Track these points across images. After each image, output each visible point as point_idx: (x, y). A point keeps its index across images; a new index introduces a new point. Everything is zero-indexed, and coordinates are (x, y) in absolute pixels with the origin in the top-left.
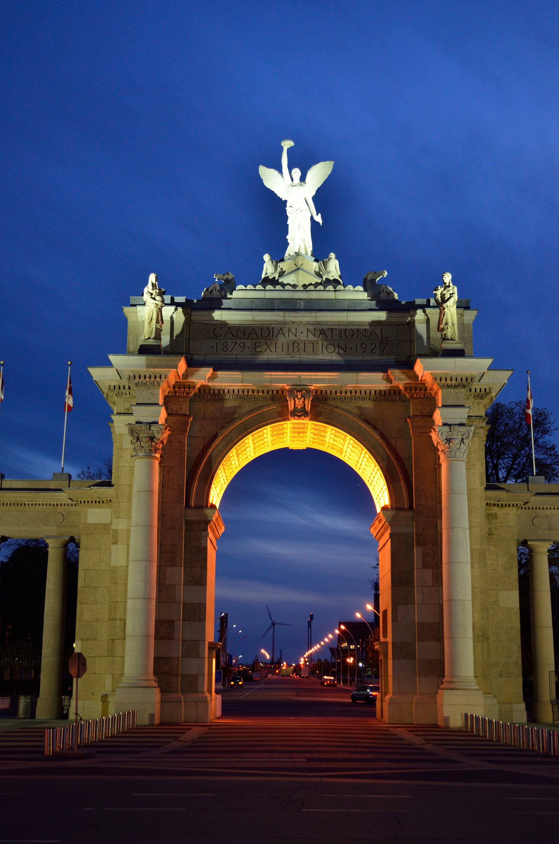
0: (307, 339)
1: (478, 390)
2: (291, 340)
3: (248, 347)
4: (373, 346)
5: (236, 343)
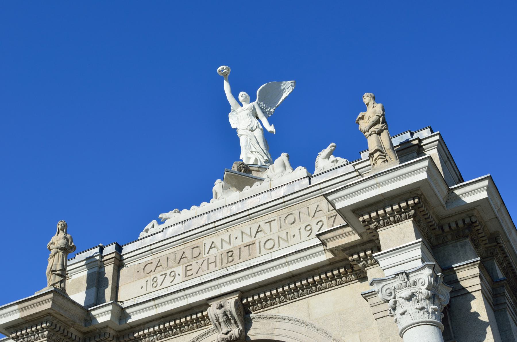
0: (242, 243)
1: (453, 226)
2: (226, 250)
3: (179, 275)
4: (320, 224)
5: (167, 273)
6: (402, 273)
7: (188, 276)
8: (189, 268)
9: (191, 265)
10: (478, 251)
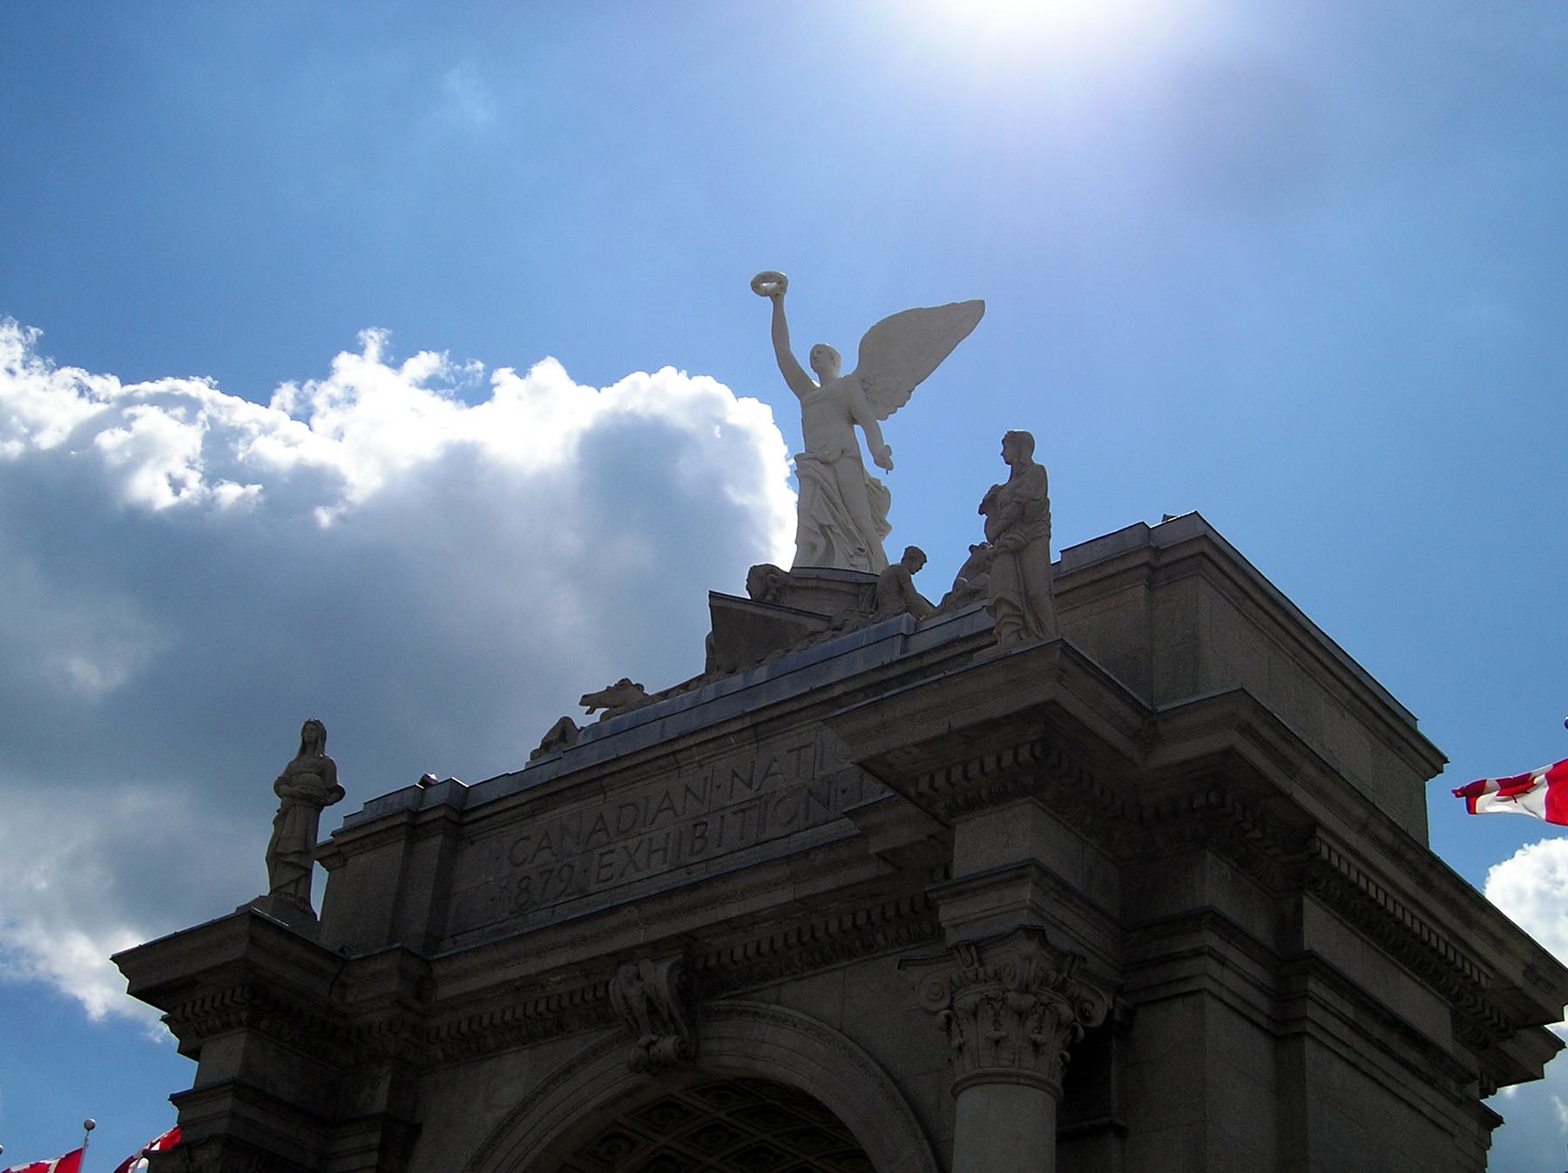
6: (968, 947)
7: (603, 881)
8: (606, 860)
9: (612, 852)
10: (1253, 874)
